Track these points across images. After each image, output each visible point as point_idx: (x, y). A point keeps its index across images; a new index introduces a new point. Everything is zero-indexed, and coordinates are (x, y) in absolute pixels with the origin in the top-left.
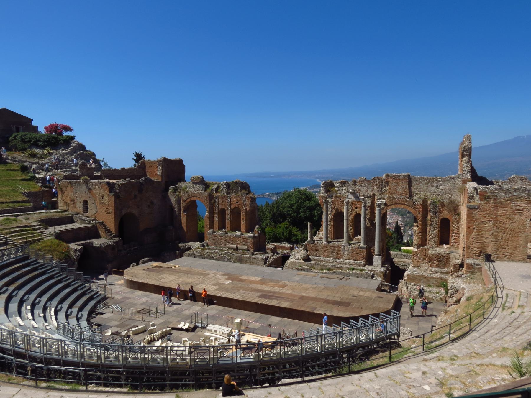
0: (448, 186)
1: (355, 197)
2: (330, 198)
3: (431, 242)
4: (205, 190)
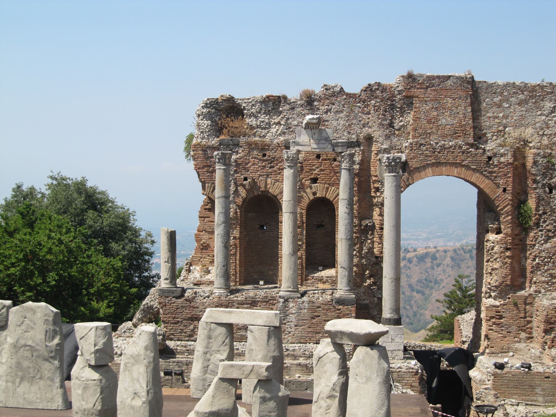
1: (318, 142)
3: (539, 277)
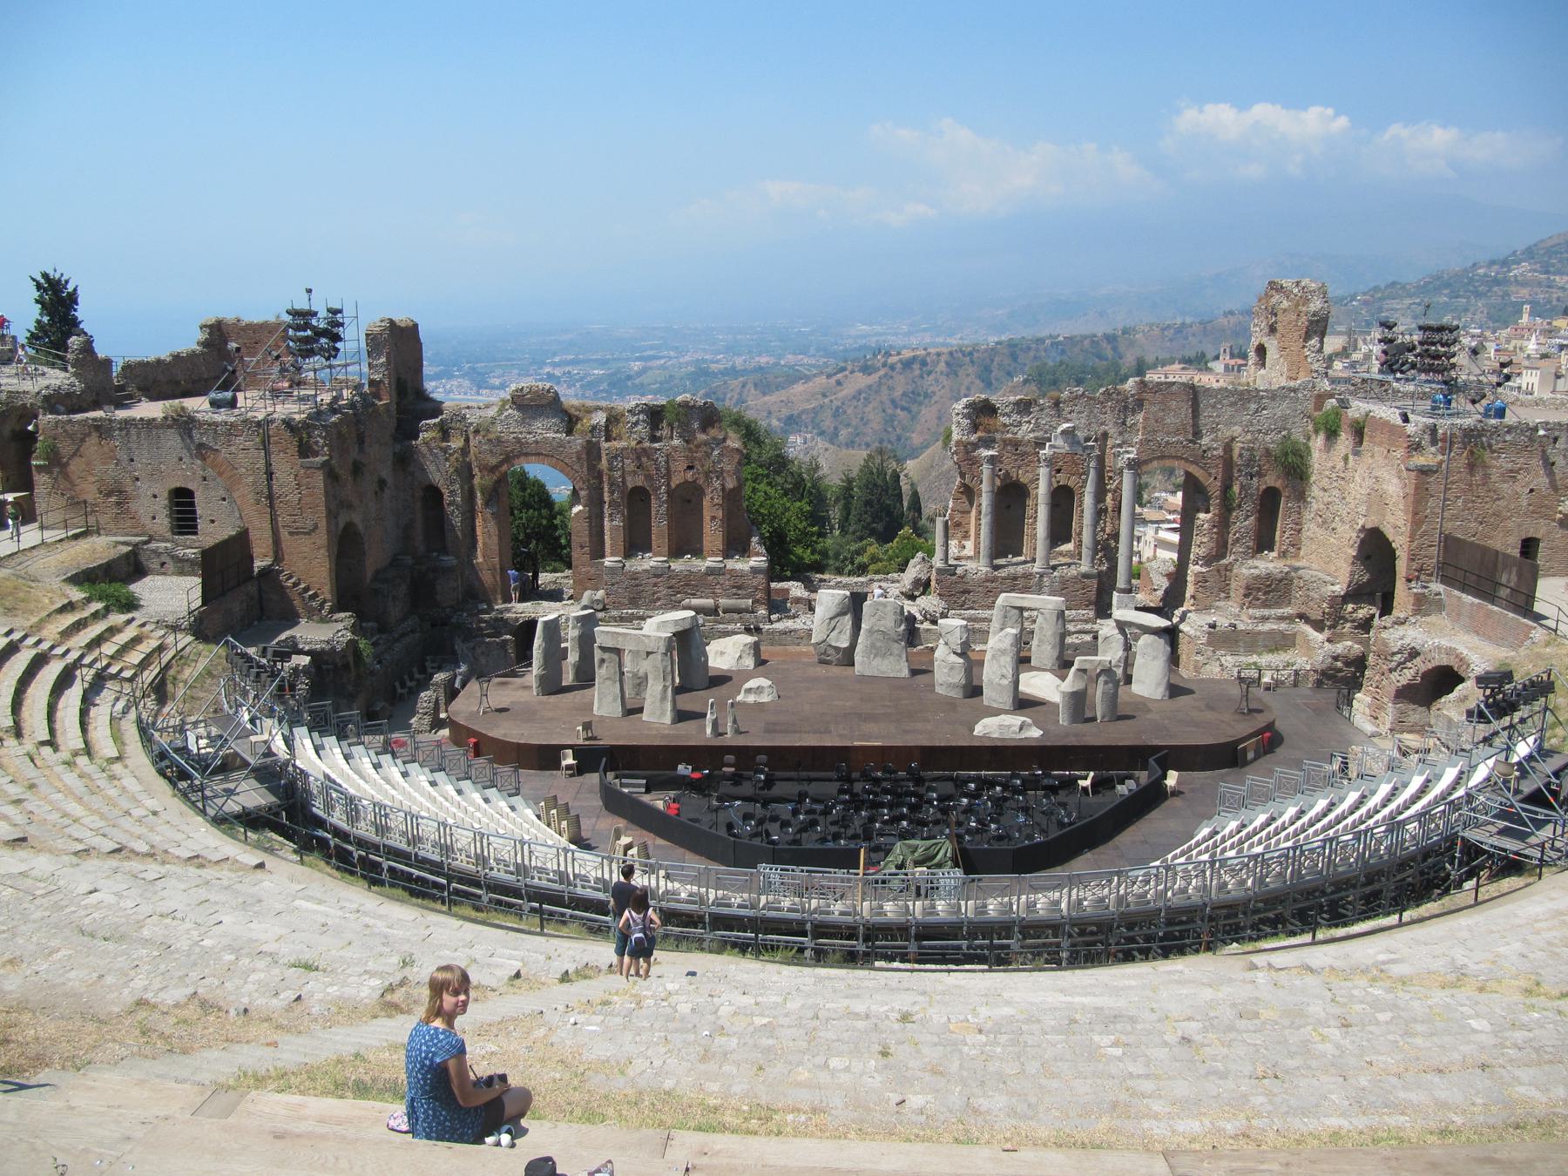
0: (1282, 408)
2: (988, 447)
3: (1238, 549)
4: (569, 432)
